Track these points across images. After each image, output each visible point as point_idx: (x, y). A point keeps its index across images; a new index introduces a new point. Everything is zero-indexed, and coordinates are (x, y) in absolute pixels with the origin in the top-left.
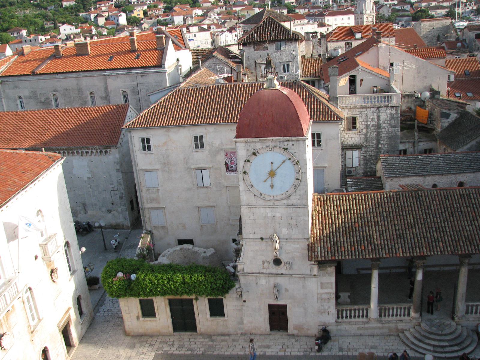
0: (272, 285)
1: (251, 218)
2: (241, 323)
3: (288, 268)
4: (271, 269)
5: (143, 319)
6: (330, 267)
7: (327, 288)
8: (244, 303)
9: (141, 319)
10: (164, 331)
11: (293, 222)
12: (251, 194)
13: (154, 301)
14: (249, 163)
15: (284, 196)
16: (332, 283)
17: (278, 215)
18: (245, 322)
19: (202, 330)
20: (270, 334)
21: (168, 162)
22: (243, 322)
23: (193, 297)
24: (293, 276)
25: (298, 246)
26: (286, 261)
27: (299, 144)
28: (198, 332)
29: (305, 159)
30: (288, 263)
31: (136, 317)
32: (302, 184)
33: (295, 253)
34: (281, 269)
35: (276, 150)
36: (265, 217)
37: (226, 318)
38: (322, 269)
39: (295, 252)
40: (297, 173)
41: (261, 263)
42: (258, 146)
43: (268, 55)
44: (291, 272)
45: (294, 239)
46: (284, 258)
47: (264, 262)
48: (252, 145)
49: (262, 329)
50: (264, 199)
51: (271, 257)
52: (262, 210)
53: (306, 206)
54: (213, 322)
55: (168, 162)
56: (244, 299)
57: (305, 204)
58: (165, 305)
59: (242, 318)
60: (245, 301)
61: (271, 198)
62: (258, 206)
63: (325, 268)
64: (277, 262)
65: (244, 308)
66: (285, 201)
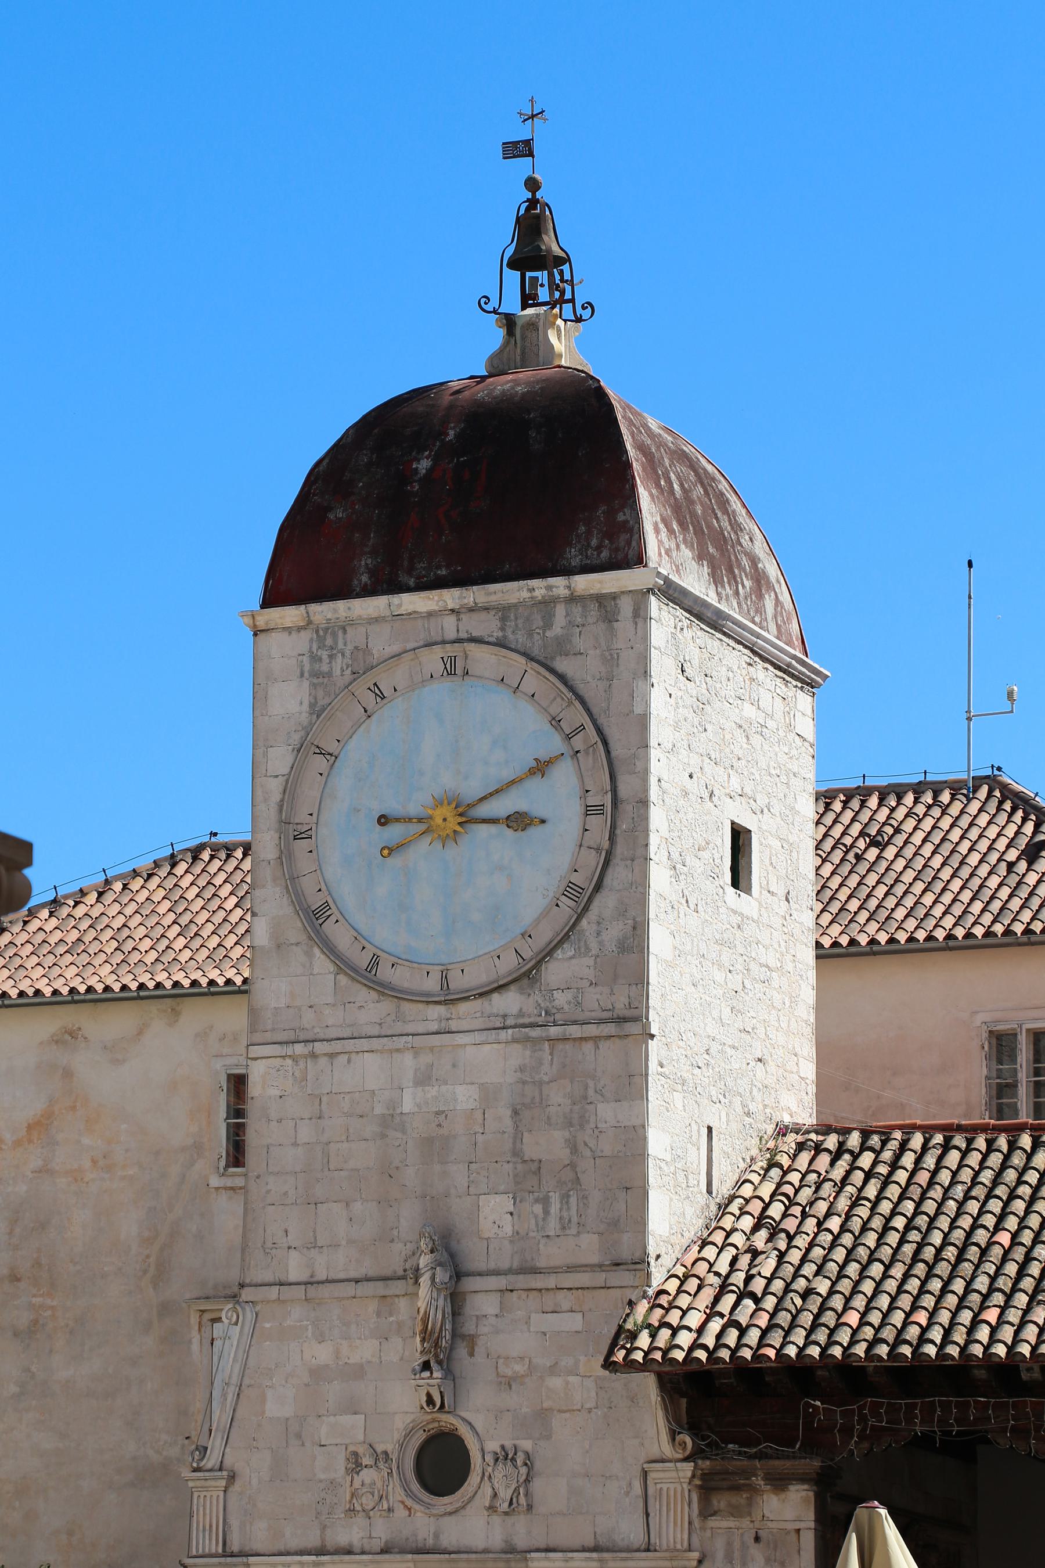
3: (505, 1494)
4: (401, 1512)
11: (548, 1144)
12: (322, 963)
15: (509, 964)
21: (37, 1264)
25: (575, 1322)
26: (493, 1446)
29: (638, 710)
33: (556, 1383)
36: (391, 1121)
39: (553, 1370)
40: (588, 811)
45: (554, 1271)
46: (483, 1423)
47: (356, 1465)
50: (384, 989)
52: (367, 1072)
53: (633, 1028)
55: (37, 1264)
57: (628, 1013)
61: (432, 984)
62: (350, 1045)
63: (741, 1499)
64: (441, 1463)
66: (509, 1002)
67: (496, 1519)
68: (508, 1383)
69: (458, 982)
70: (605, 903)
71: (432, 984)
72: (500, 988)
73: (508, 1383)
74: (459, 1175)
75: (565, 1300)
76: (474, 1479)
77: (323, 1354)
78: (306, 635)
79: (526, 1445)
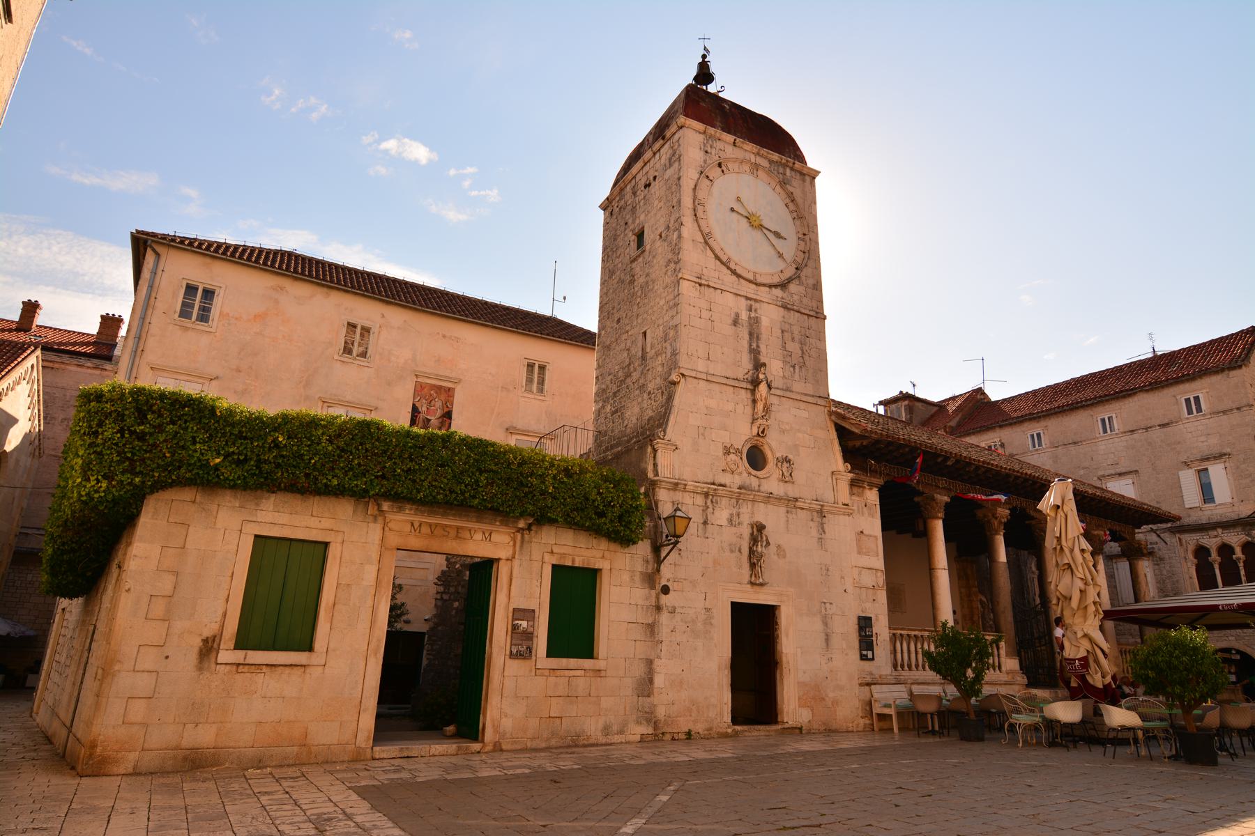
0: (746, 531)
1: (705, 314)
2: (646, 686)
4: (745, 474)
5: (239, 656)
6: (871, 486)
7: (867, 554)
8: (663, 597)
9: (227, 655)
10: (326, 735)
12: (709, 253)
13: (333, 551)
14: (708, 182)
15: (776, 280)
16: (876, 537)
17: (765, 322)
18: (659, 681)
19: (507, 724)
20: (736, 734)
22: (651, 681)
23: (502, 553)
24: (798, 504)
25: (805, 414)
26: (779, 455)
27: (804, 181)
28: (489, 735)
30: (787, 460)
31: (197, 642)
32: (811, 263)
33: (800, 435)
34: (770, 481)
35: (760, 173)
37: (600, 664)
38: (855, 490)
41: (720, 452)
42: (730, 152)
43: (704, 57)
44: (792, 491)
46: (774, 446)
47: (727, 452)
48: (719, 145)
49: (712, 714)
50: (734, 272)
51: (742, 434)
54: (552, 679)
56: (664, 582)
58: (378, 582)
59: (650, 662)
60: (666, 590)
64: (756, 458)
65: (664, 618)
67: (781, 484)
68: (783, 432)
69: (760, 280)
70: (806, 272)
71: (750, 277)
72: (776, 286)
73: (783, 432)
74: (763, 348)
75: (802, 405)
76: (771, 465)
77: (712, 403)
78: (702, 136)
79: (790, 457)
